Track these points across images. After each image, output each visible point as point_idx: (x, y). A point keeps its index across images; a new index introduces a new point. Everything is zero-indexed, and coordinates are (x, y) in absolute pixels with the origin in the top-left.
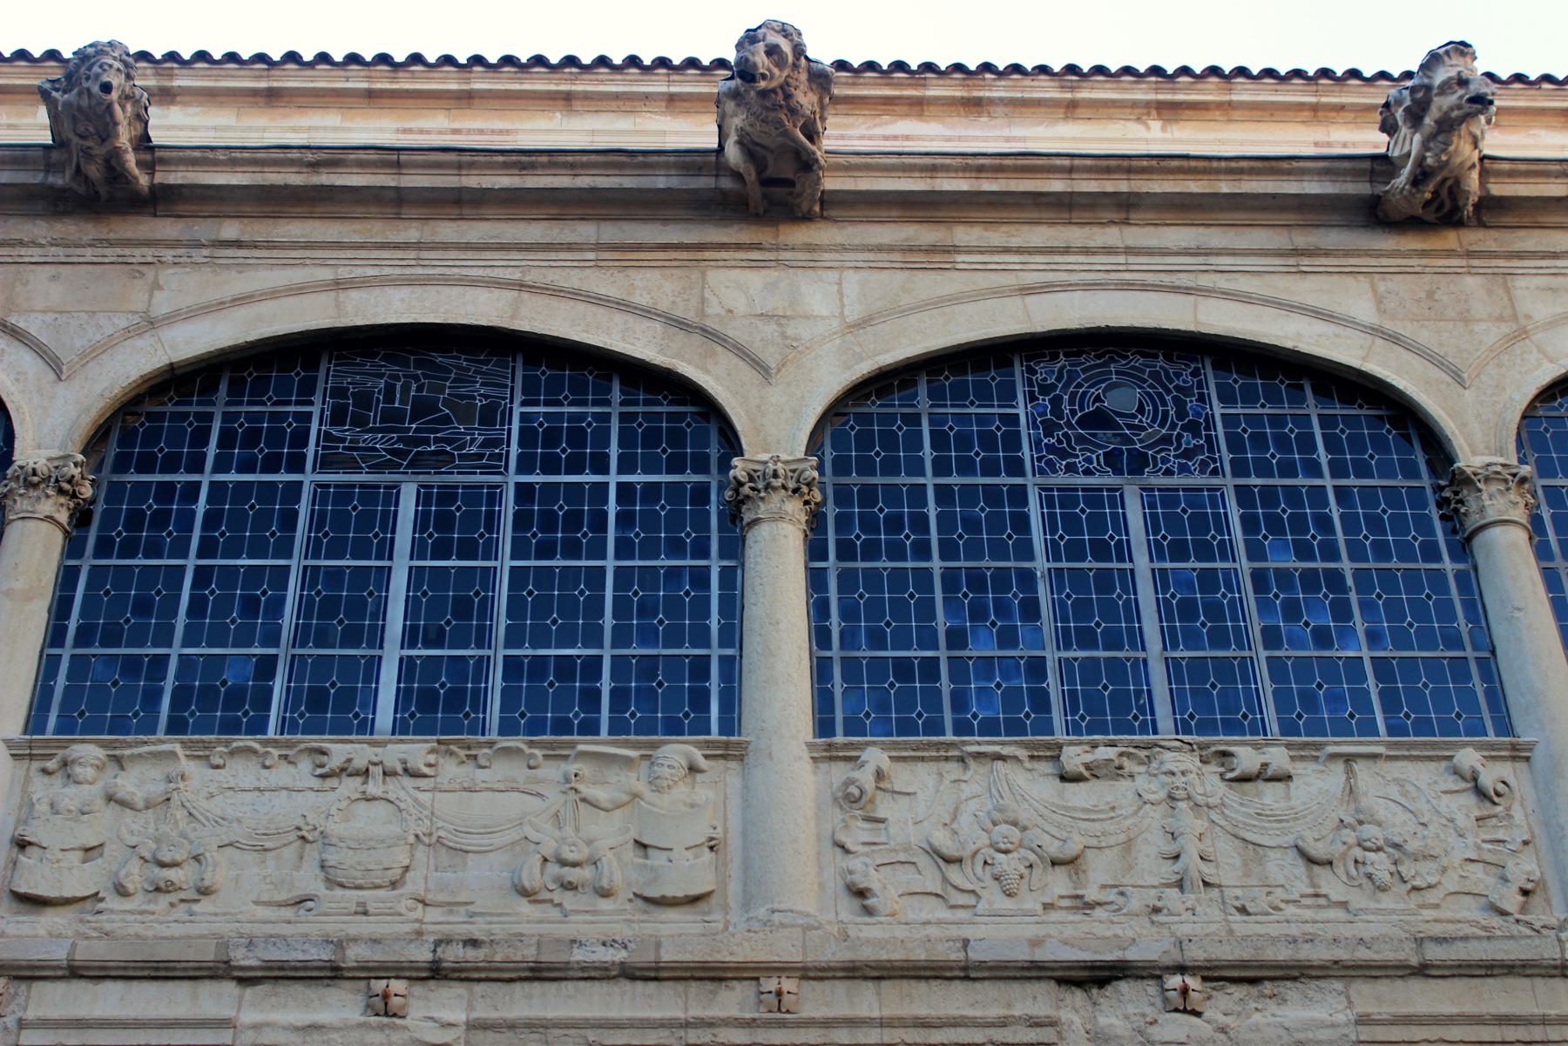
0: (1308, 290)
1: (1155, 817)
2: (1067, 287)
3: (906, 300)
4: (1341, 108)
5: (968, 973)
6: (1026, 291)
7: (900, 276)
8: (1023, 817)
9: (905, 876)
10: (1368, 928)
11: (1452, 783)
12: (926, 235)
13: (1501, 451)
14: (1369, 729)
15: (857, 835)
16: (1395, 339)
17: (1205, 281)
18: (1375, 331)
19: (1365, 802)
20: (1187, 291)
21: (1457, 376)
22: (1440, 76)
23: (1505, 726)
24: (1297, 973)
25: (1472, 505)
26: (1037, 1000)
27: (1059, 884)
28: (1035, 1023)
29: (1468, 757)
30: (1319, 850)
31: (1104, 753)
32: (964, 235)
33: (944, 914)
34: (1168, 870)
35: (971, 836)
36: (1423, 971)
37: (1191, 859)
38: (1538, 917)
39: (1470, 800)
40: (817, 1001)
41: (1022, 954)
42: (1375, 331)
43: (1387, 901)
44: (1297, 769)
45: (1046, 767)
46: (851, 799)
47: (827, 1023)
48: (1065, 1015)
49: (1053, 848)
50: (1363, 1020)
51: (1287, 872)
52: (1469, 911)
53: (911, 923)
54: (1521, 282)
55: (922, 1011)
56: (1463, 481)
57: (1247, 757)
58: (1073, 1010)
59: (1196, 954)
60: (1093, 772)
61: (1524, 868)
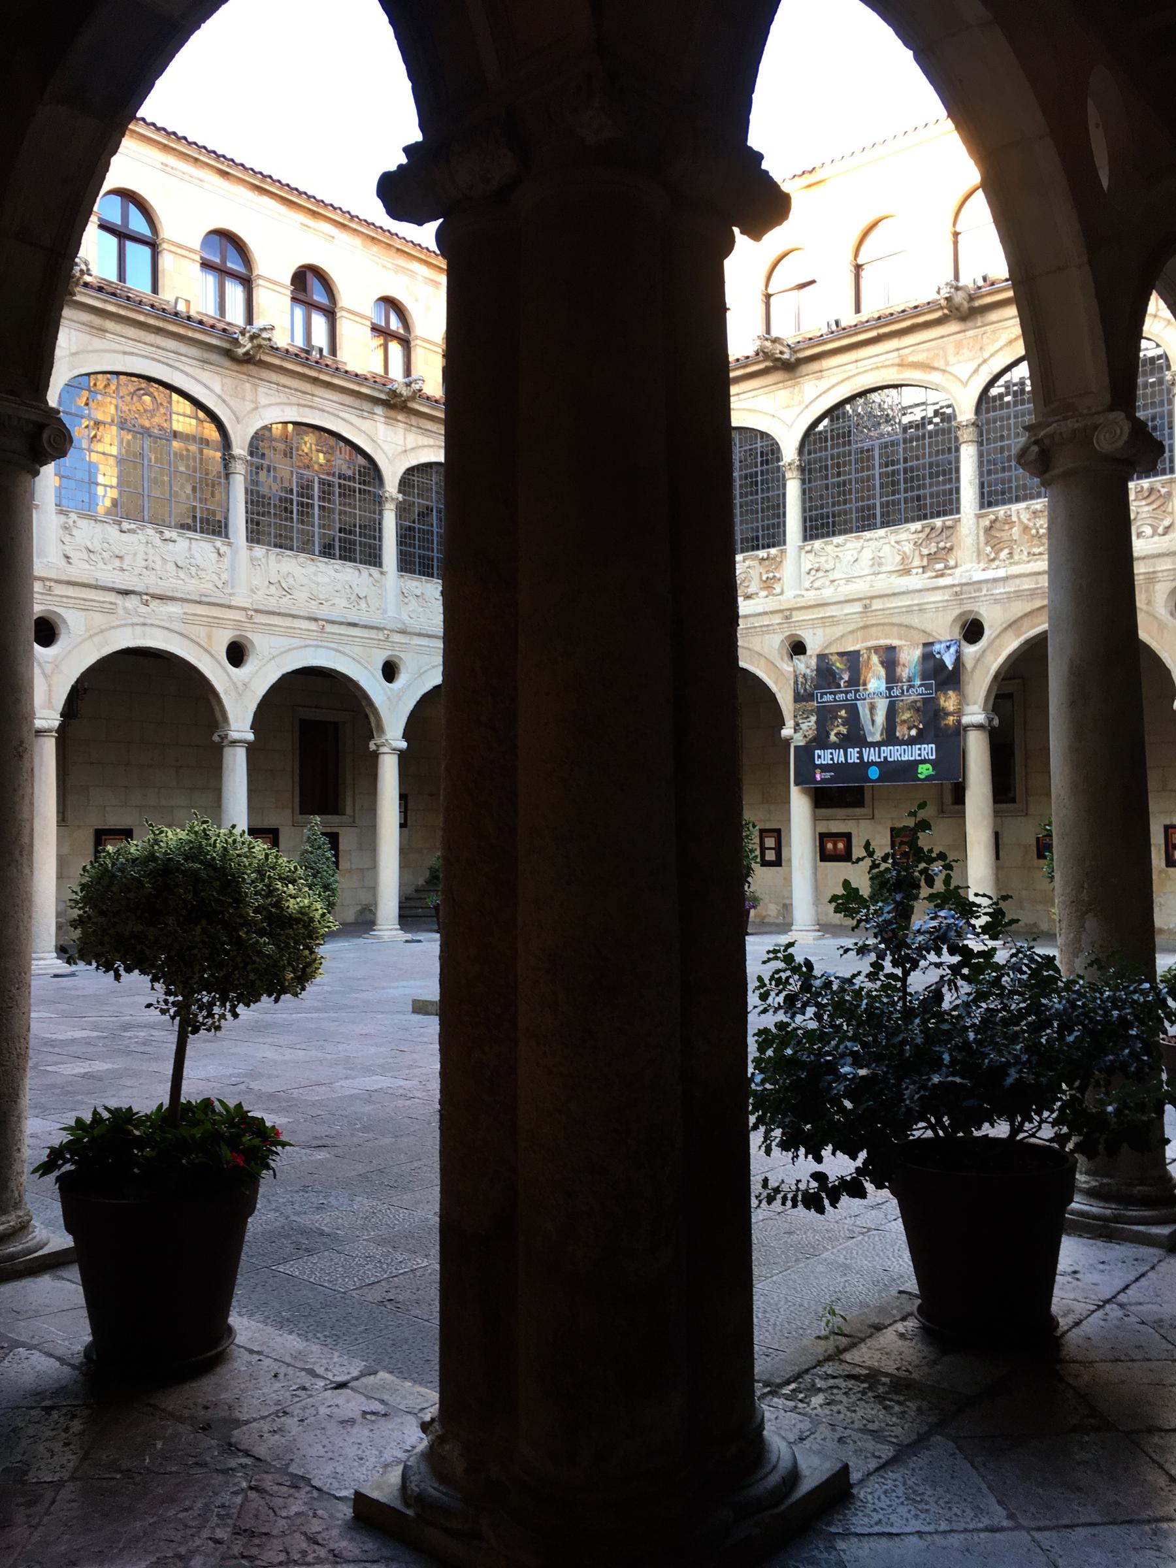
0: (206, 376)
1: (142, 548)
2: (137, 355)
3: (90, 348)
4: (175, 149)
5: (96, 587)
6: (125, 353)
7: (89, 337)
8: (111, 542)
9: (79, 554)
10: (189, 588)
11: (213, 550)
12: (97, 321)
13: (243, 449)
14: (195, 531)
15: (67, 539)
16: (224, 401)
17: (177, 364)
18: (219, 397)
19: (193, 552)
20: (171, 366)
21: (237, 418)
22: (265, 335)
23: (227, 536)
24: (172, 599)
25: (233, 465)
26: (111, 597)
27: (117, 563)
28: (111, 603)
29: (218, 544)
30: (180, 564)
31: (133, 526)
32: (110, 325)
33: (88, 567)
34: (144, 564)
35: (96, 546)
36: (200, 603)
37: (150, 561)
38: (226, 591)
39: (216, 555)
40: (59, 590)
41: (111, 585)
42: (219, 397)
43: (193, 581)
44: (178, 539)
45: (116, 527)
46: (66, 528)
47: (62, 596)
48: (118, 602)
49: (117, 552)
50: (185, 613)
51: (171, 567)
52: (210, 586)
53: (80, 570)
54: (260, 389)
55: (84, 596)
56: (233, 457)
57: (168, 534)
58: (119, 600)
59: (151, 591)
60: (129, 531)
61: (225, 576)
